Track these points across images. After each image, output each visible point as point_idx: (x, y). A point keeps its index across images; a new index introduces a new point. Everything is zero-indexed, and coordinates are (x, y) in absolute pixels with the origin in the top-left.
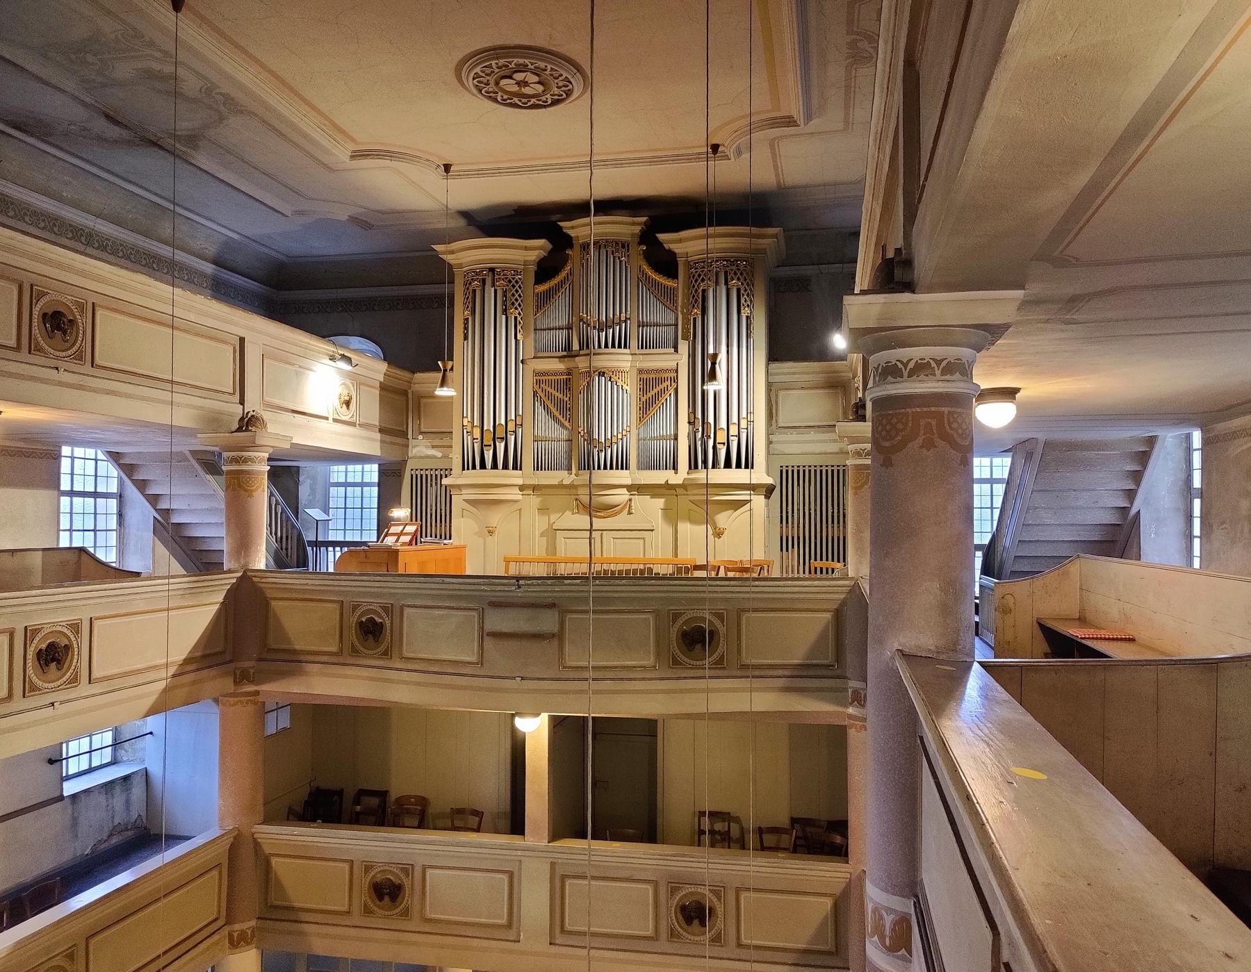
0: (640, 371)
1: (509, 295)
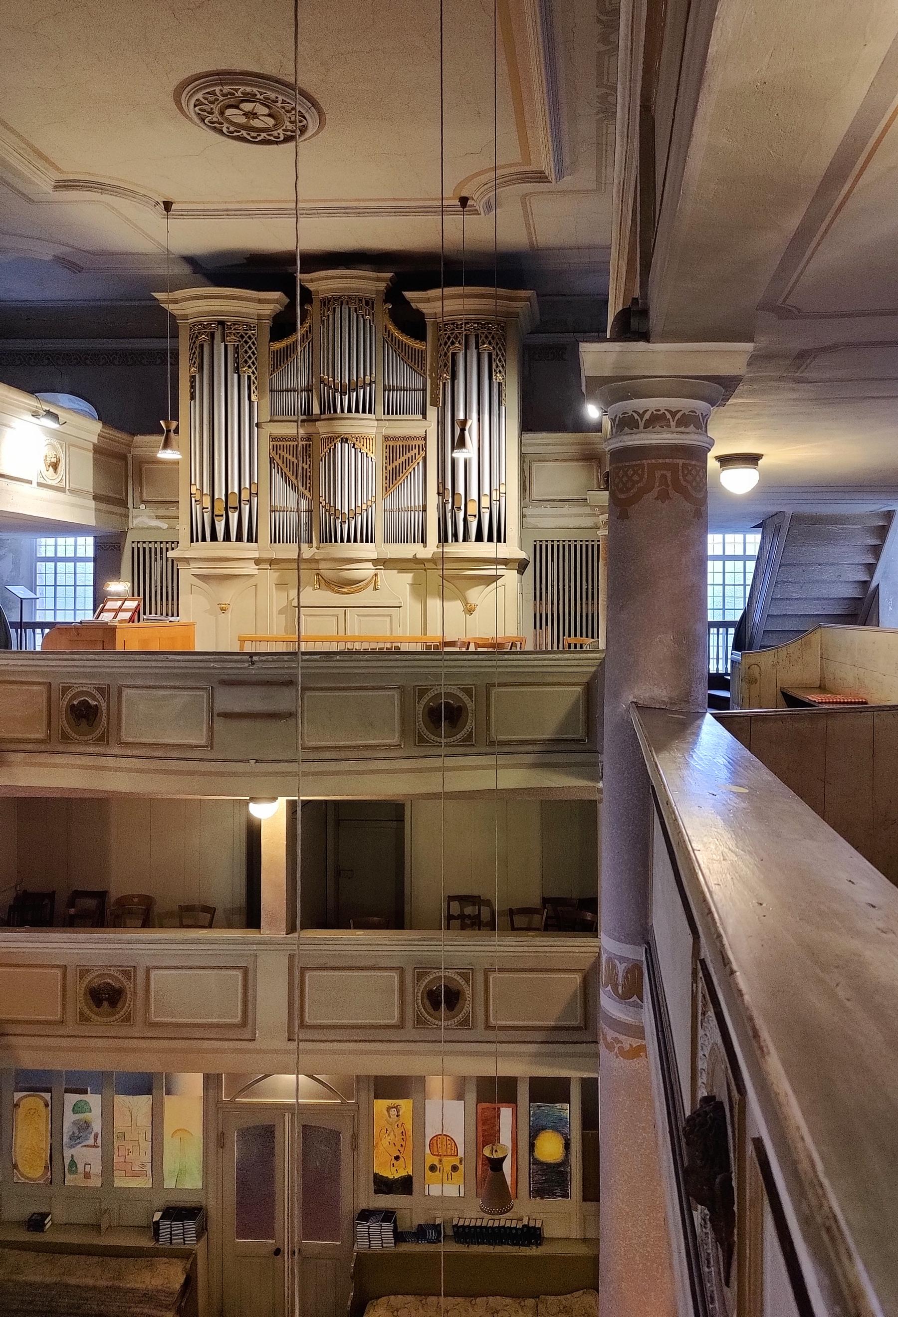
0: (386, 438)
1: (241, 352)
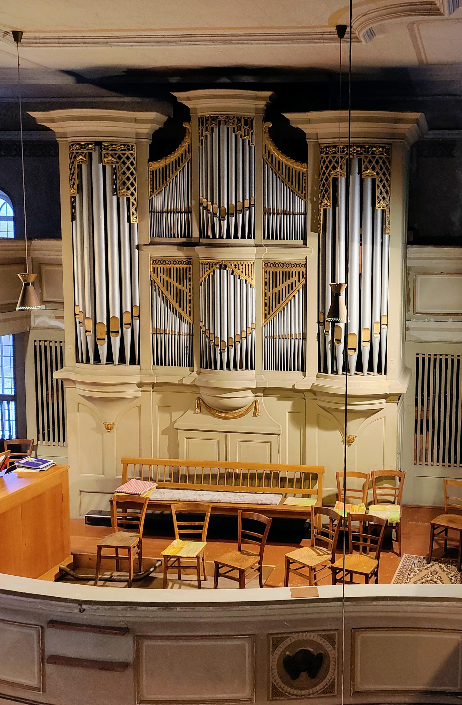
0: (266, 264)
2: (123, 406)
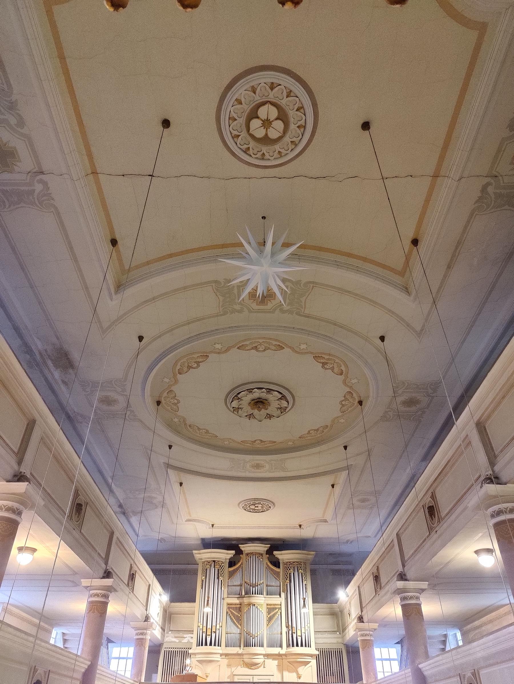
0: (267, 605)
1: (220, 571)
2: (213, 665)
